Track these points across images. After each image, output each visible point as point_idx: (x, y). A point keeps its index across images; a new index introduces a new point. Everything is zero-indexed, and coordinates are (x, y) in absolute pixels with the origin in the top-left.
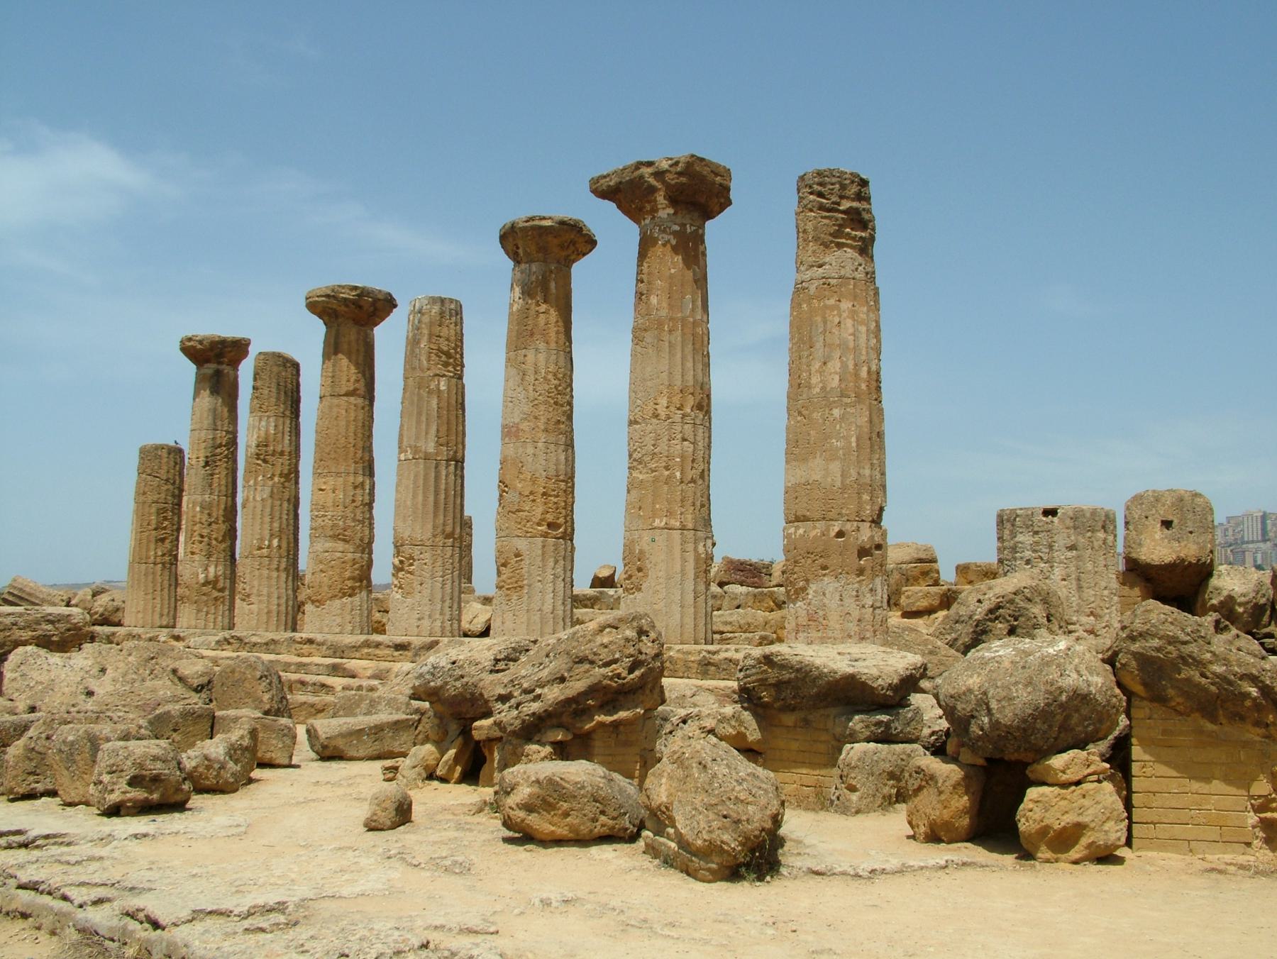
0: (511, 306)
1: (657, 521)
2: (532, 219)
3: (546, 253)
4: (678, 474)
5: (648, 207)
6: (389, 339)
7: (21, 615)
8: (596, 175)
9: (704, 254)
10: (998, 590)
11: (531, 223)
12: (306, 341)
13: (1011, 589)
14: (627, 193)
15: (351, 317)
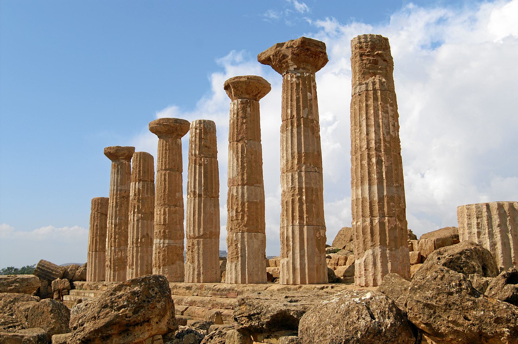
0: (230, 121)
1: (295, 221)
2: (237, 77)
3: (247, 93)
4: (304, 197)
5: (284, 66)
6: (186, 140)
7: (5, 279)
8: (260, 53)
9: (315, 87)
10: (450, 252)
11: (236, 80)
12: (150, 144)
13: (457, 251)
14: (275, 61)
15: (170, 131)
